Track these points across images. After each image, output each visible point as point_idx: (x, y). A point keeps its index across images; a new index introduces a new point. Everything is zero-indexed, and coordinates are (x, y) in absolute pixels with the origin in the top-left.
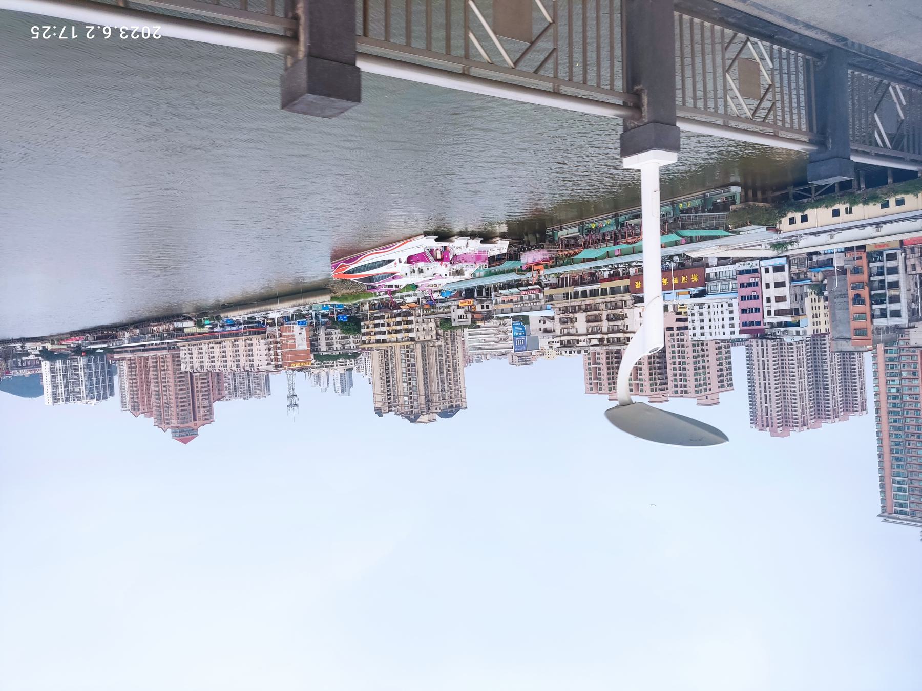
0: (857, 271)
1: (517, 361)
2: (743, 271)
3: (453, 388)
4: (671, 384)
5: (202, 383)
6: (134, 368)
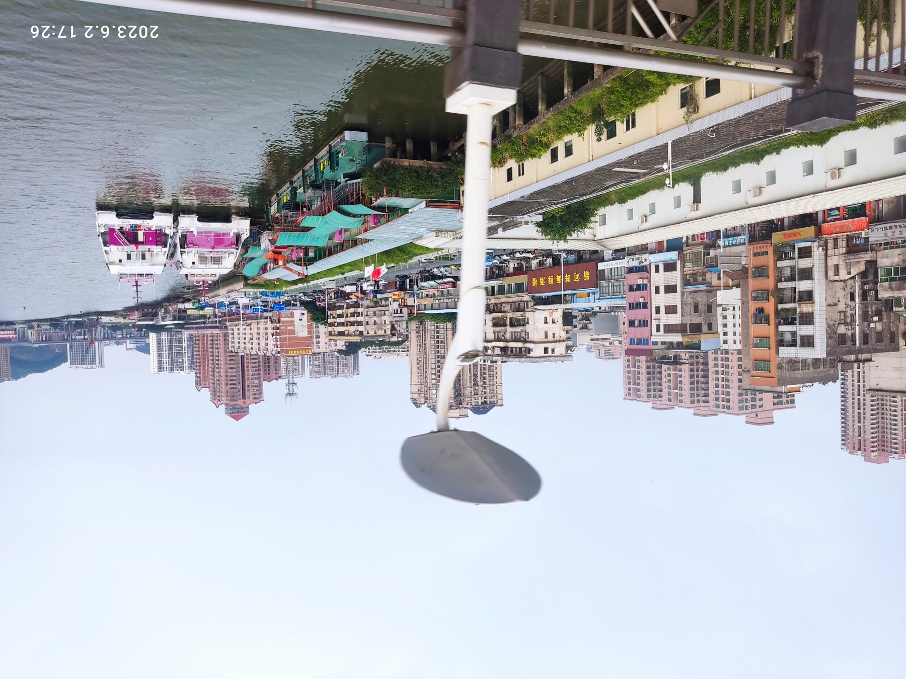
0: (761, 272)
1: (603, 354)
2: (632, 268)
3: (488, 383)
4: (712, 396)
5: (252, 363)
6: (198, 344)
